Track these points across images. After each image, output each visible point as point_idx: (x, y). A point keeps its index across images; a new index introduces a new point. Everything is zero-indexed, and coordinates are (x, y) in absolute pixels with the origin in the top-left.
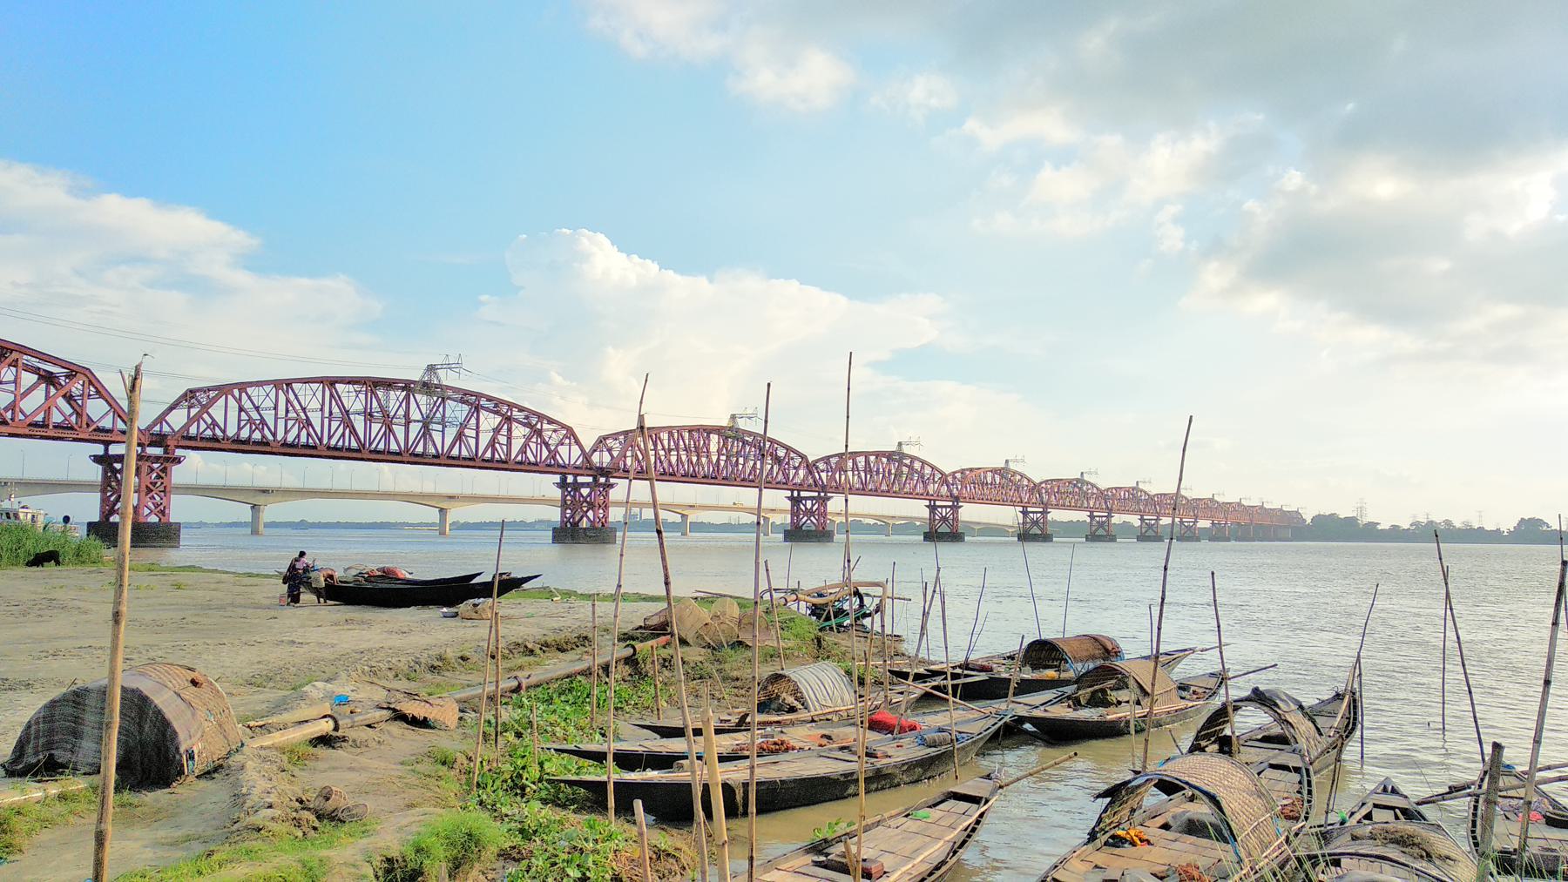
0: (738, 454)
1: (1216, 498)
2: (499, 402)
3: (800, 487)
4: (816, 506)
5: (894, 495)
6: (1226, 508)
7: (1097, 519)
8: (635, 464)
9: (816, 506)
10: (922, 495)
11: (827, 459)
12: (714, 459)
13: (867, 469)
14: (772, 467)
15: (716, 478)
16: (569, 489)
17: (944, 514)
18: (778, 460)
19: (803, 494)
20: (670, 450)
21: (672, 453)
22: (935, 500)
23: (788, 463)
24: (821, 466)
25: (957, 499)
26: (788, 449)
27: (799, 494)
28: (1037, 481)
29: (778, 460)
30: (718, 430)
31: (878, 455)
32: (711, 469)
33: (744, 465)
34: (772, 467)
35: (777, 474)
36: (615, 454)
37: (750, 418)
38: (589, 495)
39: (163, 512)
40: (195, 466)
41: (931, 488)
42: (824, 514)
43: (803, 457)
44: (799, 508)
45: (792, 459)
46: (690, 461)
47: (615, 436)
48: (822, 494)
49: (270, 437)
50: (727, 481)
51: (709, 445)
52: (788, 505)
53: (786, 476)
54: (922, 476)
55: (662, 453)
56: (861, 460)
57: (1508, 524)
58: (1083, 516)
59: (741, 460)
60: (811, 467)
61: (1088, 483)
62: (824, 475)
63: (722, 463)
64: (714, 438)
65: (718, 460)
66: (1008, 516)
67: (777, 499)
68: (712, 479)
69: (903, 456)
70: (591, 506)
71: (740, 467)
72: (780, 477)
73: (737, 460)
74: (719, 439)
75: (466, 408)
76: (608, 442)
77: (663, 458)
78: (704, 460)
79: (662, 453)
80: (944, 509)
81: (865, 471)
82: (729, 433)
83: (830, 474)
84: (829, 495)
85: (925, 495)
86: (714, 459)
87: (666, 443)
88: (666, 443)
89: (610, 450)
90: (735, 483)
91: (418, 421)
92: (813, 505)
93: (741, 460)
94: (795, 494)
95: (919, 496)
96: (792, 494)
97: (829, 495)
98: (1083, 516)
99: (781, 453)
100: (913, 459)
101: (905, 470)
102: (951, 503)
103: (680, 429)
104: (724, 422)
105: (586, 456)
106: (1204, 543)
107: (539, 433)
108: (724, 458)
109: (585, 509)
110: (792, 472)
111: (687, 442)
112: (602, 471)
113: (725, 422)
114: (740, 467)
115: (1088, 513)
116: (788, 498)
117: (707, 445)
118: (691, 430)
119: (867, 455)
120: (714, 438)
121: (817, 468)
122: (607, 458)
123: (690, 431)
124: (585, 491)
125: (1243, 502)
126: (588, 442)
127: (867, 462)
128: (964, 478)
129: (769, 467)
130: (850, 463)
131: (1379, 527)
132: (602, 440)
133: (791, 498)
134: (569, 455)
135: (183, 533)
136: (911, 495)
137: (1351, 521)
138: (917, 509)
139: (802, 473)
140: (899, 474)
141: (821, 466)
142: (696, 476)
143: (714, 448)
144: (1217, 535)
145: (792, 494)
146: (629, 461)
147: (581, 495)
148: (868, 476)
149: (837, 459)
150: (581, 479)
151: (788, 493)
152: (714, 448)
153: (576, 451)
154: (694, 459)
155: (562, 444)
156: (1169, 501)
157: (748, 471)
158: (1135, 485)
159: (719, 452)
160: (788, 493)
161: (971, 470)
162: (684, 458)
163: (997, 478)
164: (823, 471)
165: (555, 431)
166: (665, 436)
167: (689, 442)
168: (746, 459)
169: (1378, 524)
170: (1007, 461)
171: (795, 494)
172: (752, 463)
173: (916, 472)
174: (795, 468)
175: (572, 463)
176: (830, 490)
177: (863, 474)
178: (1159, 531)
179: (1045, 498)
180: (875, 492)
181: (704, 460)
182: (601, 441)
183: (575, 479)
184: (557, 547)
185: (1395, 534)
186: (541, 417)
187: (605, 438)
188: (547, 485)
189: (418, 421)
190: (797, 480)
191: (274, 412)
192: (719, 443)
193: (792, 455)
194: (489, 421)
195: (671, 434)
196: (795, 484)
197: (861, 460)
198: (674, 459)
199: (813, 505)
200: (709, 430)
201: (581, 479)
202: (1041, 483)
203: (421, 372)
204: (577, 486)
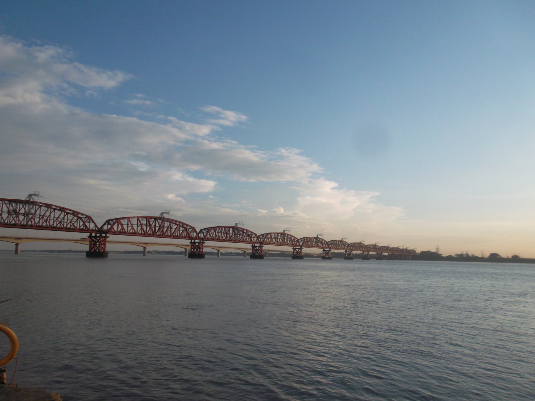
0: (237, 234)
1: (399, 247)
2: (176, 221)
3: (255, 243)
4: (259, 248)
5: (234, 242)
6: (393, 249)
7: (365, 253)
8: (210, 237)
9: (259, 248)
10: (291, 245)
11: (262, 235)
12: (231, 235)
13: (275, 238)
14: (247, 238)
15: (231, 240)
17: (298, 251)
18: (248, 235)
19: (256, 245)
20: (219, 233)
21: (214, 234)
22: (295, 247)
23: (251, 236)
24: (261, 237)
25: (301, 246)
26: (251, 232)
27: (254, 245)
28: (349, 243)
29: (248, 235)
30: (233, 228)
31: (278, 234)
32: (230, 238)
33: (239, 237)
34: (247, 238)
35: (248, 239)
36: (205, 234)
37: (241, 224)
38: (198, 245)
39: (105, 250)
40: (111, 237)
41: (294, 243)
42: (262, 251)
43: (256, 235)
44: (254, 248)
45: (253, 235)
46: (224, 236)
47: (205, 229)
48: (201, 241)
49: (62, 226)
50: (234, 241)
52: (251, 248)
53: (251, 240)
54: (291, 239)
55: (217, 234)
56: (273, 235)
57: (487, 255)
58: (343, 251)
59: (238, 236)
60: (258, 237)
61: (363, 244)
62: (262, 240)
63: (233, 236)
64: (231, 229)
65: (232, 236)
66: (319, 251)
67: (249, 246)
68: (229, 241)
69: (319, 238)
70: (199, 248)
71: (243, 239)
72: (249, 240)
73: (237, 236)
75: (169, 223)
77: (217, 235)
78: (228, 236)
79: (217, 234)
80: (298, 250)
81: (274, 238)
82: (235, 228)
83: (263, 239)
84: (204, 241)
85: (293, 245)
86: (231, 235)
88: (218, 231)
89: (203, 233)
90: (162, 237)
91: (158, 227)
92: (258, 248)
93: (238, 236)
94: (254, 245)
95: (249, 243)
96: (253, 245)
97: (204, 241)
98: (343, 251)
99: (250, 233)
100: (288, 235)
101: (286, 238)
102: (300, 248)
103: (222, 227)
104: (233, 225)
105: (198, 234)
106: (385, 261)
107: (186, 229)
108: (233, 235)
110: (253, 239)
112: (202, 239)
114: (243, 239)
115: (345, 251)
116: (251, 246)
117: (229, 231)
118: (225, 227)
119: (275, 234)
120: (231, 229)
121: (260, 237)
122: (202, 235)
123: (224, 228)
124: (197, 244)
125: (407, 249)
126: (198, 231)
127: (275, 235)
128: (304, 240)
129: (246, 237)
130: (269, 236)
131: (442, 256)
132: (201, 231)
133: (252, 246)
134: (194, 235)
135: (109, 255)
136: (288, 245)
137: (434, 253)
138: (290, 249)
139: (255, 239)
140: (284, 239)
141: (261, 237)
142: (226, 240)
143: (231, 232)
144: (390, 258)
145: (253, 245)
146: (208, 236)
147: (196, 245)
148: (275, 240)
149: (265, 235)
150: (196, 241)
151: (252, 245)
152: (231, 232)
153: (195, 234)
154: (226, 235)
155: (192, 232)
156: (358, 245)
157: (240, 239)
158: (360, 242)
159: (232, 234)
160: (252, 245)
161: (333, 241)
162: (223, 235)
163: (339, 242)
164: (261, 238)
165: (190, 228)
166: (218, 229)
169: (442, 255)
170: (317, 235)
171: (254, 245)
172: (241, 236)
173: (289, 238)
174: (254, 238)
175: (138, 232)
176: (205, 240)
177: (273, 239)
178: (352, 256)
179: (351, 248)
180: (277, 244)
181: (228, 236)
183: (194, 241)
184: (189, 258)
185: (450, 258)
186: (187, 225)
188: (187, 242)
189: (158, 227)
190: (254, 241)
191: (136, 226)
193: (253, 234)
194: (174, 226)
195: (219, 229)
196: (253, 242)
197: (273, 235)
198: (220, 235)
199: (258, 248)
200: (230, 227)
201: (196, 241)
202: (350, 244)
203: (159, 215)
204: (195, 243)
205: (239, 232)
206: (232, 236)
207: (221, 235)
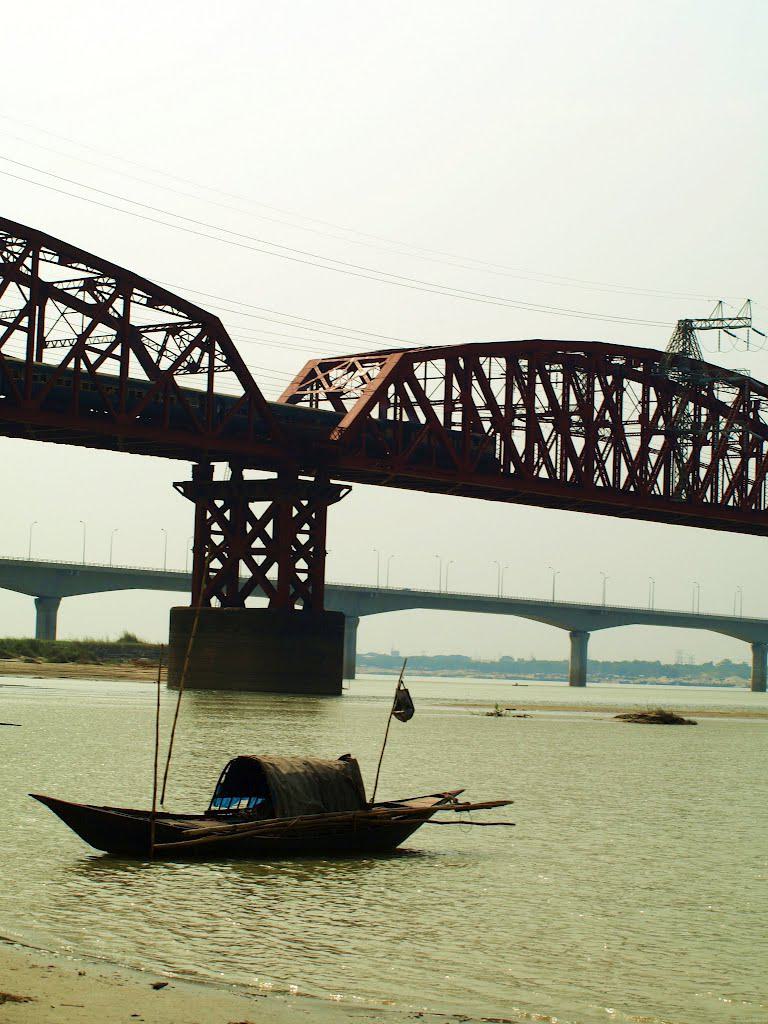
12: (634, 444)
16: (219, 503)
46: (567, 448)
51: (620, 401)
65: (645, 450)
71: (703, 472)
73: (696, 454)
74: (646, 393)
76: (334, 373)
86: (634, 444)
87: (498, 388)
109: (260, 559)
111: (558, 391)
113: (660, 339)
114: (703, 472)
117: (614, 406)
124: (259, 508)
143: (630, 410)
150: (249, 475)
167: (566, 395)
168: (719, 453)
182: (312, 374)
187: (326, 366)
192: (645, 402)
201: (249, 475)
205: (713, 420)
206: (645, 450)
207: (533, 435)
